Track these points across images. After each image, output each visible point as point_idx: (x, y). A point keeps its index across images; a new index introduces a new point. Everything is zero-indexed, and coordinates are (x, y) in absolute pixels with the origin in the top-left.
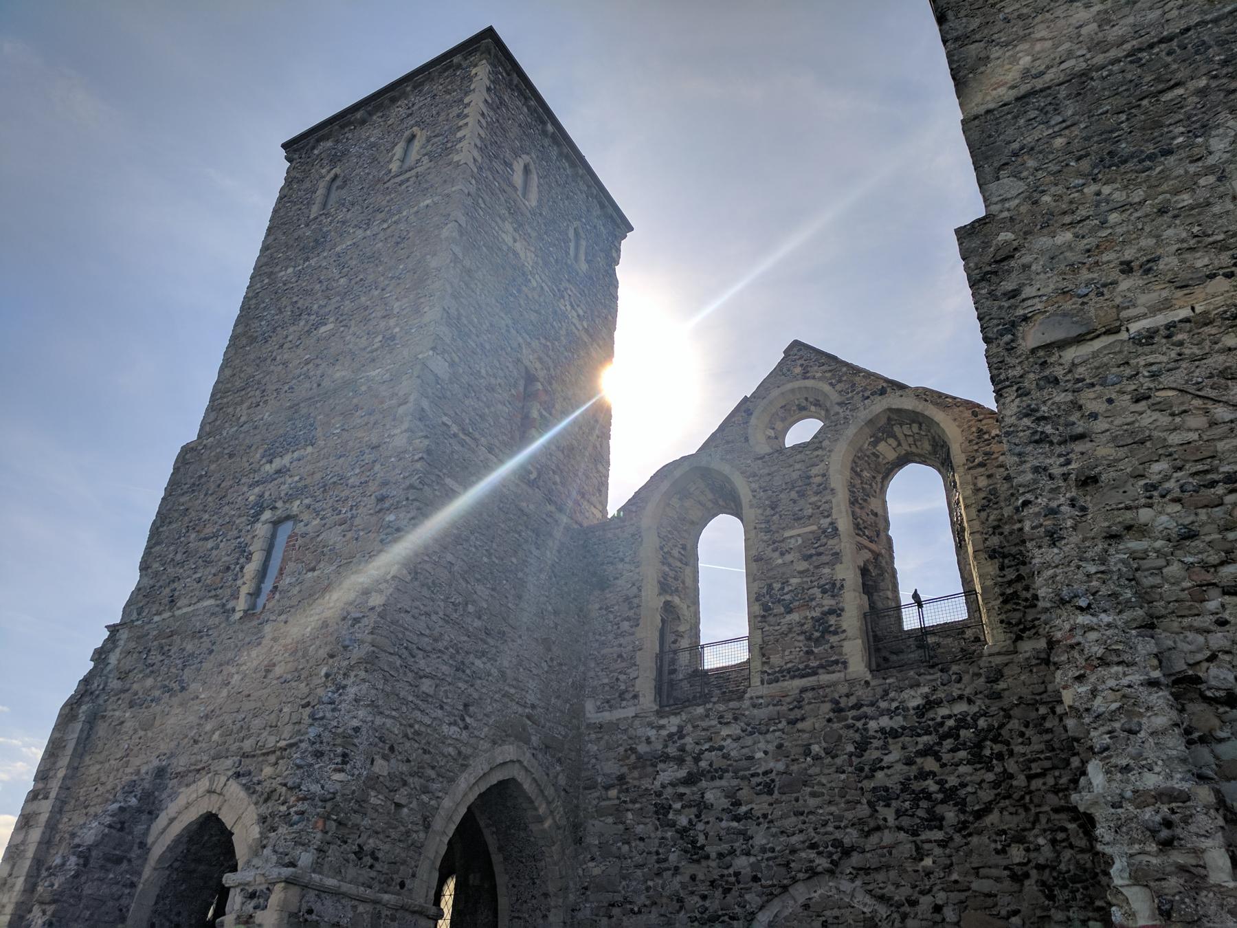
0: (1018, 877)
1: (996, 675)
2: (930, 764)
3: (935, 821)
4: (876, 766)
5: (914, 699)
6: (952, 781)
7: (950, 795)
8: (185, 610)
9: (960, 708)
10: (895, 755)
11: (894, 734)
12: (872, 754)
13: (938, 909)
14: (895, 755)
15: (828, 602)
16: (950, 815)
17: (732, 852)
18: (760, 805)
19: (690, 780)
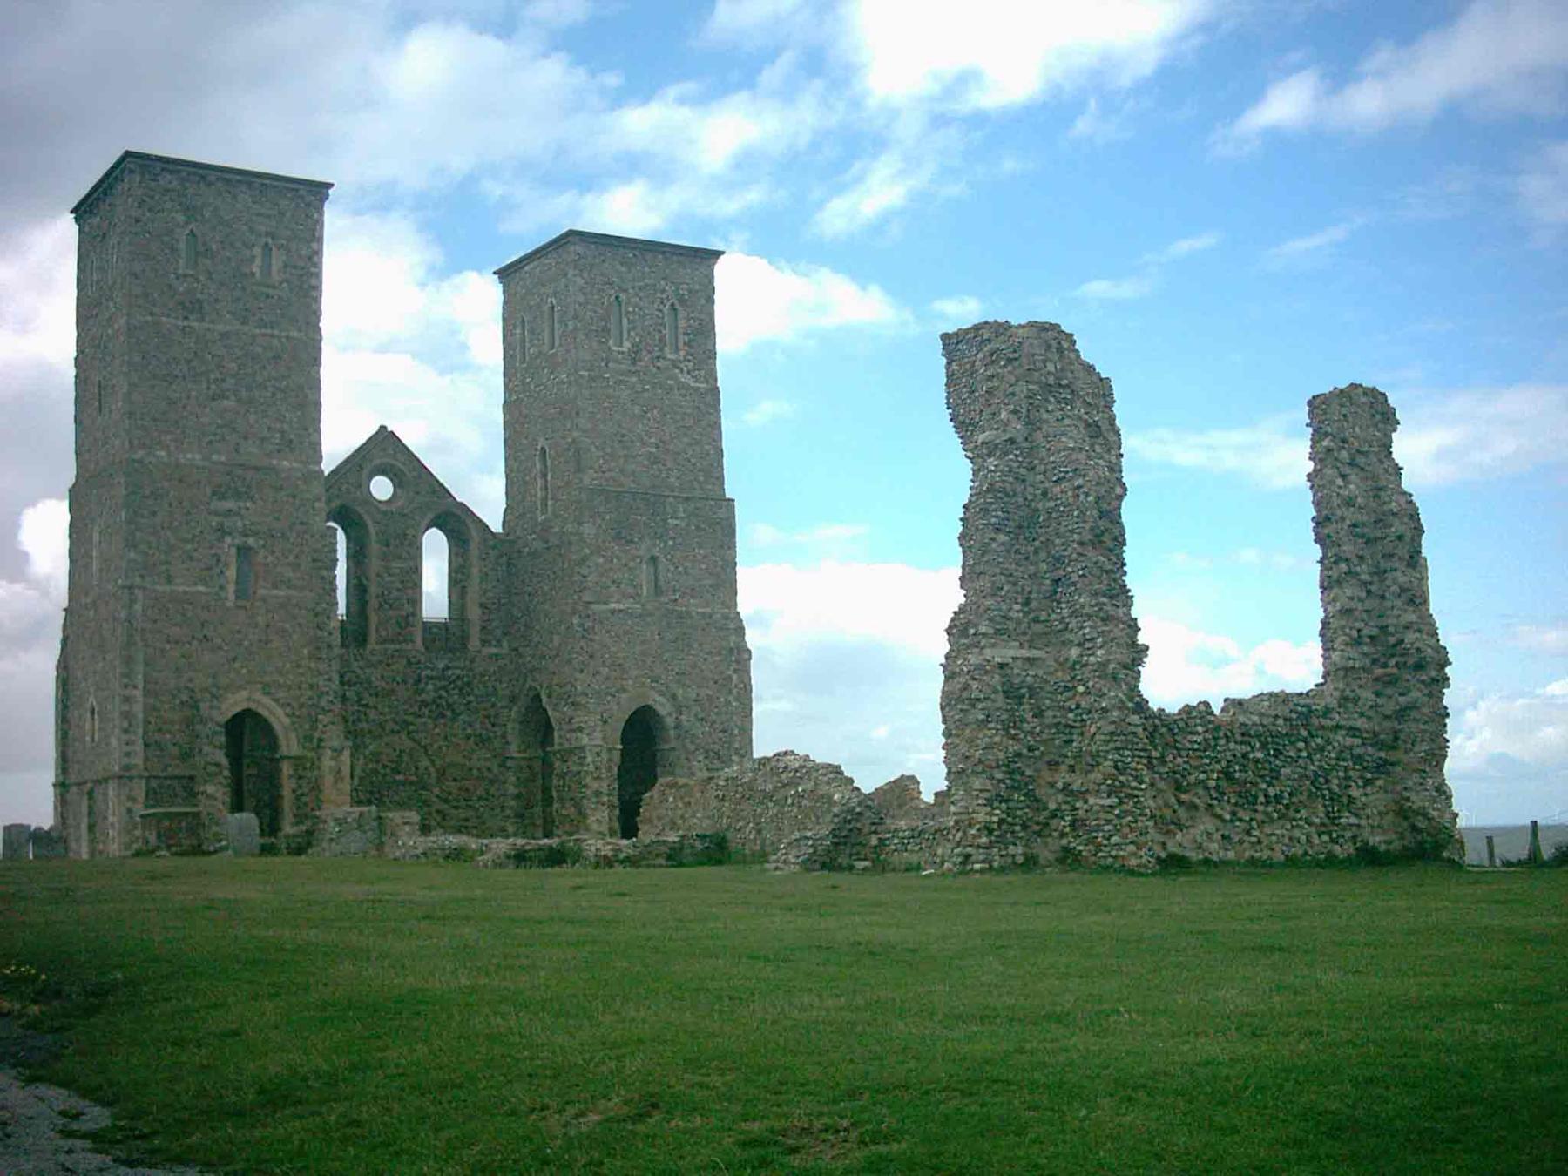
0: (468, 737)
1: (472, 661)
2: (443, 693)
3: (443, 716)
4: (423, 691)
5: (441, 665)
7: (449, 706)
8: (181, 589)
9: (458, 672)
10: (430, 687)
11: (432, 678)
12: (422, 685)
14: (430, 687)
15: (408, 608)
16: (449, 713)
17: (359, 720)
18: (372, 701)
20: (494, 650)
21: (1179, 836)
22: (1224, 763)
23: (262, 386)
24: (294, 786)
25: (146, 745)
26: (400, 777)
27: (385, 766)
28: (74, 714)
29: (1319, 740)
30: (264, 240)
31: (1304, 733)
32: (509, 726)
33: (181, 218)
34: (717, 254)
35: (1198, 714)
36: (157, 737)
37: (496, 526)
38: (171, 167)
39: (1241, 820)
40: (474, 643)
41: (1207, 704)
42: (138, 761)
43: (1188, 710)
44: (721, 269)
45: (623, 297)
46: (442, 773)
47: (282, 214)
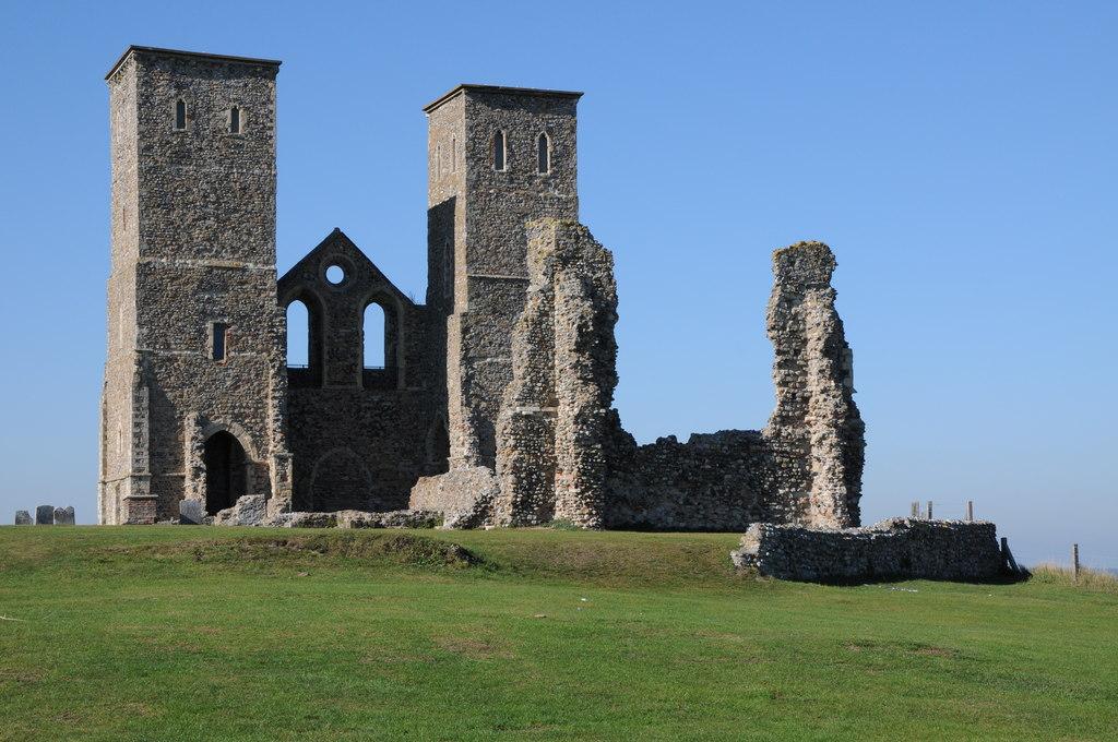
2: (378, 418)
3: (378, 435)
6: (383, 425)
13: (375, 457)
19: (302, 413)
20: (416, 389)
21: (645, 513)
22: (681, 471)
23: (235, 210)
24: (254, 483)
25: (152, 455)
26: (346, 478)
27: (334, 470)
28: (110, 434)
29: (755, 459)
30: (232, 104)
31: (744, 454)
32: (428, 442)
33: (173, 92)
34: (578, 96)
35: (667, 444)
36: (159, 450)
37: (420, 299)
38: (161, 55)
39: (691, 504)
40: (402, 384)
41: (673, 438)
42: (145, 464)
43: (660, 440)
44: (581, 105)
45: (504, 132)
46: (376, 475)
47: (246, 85)
